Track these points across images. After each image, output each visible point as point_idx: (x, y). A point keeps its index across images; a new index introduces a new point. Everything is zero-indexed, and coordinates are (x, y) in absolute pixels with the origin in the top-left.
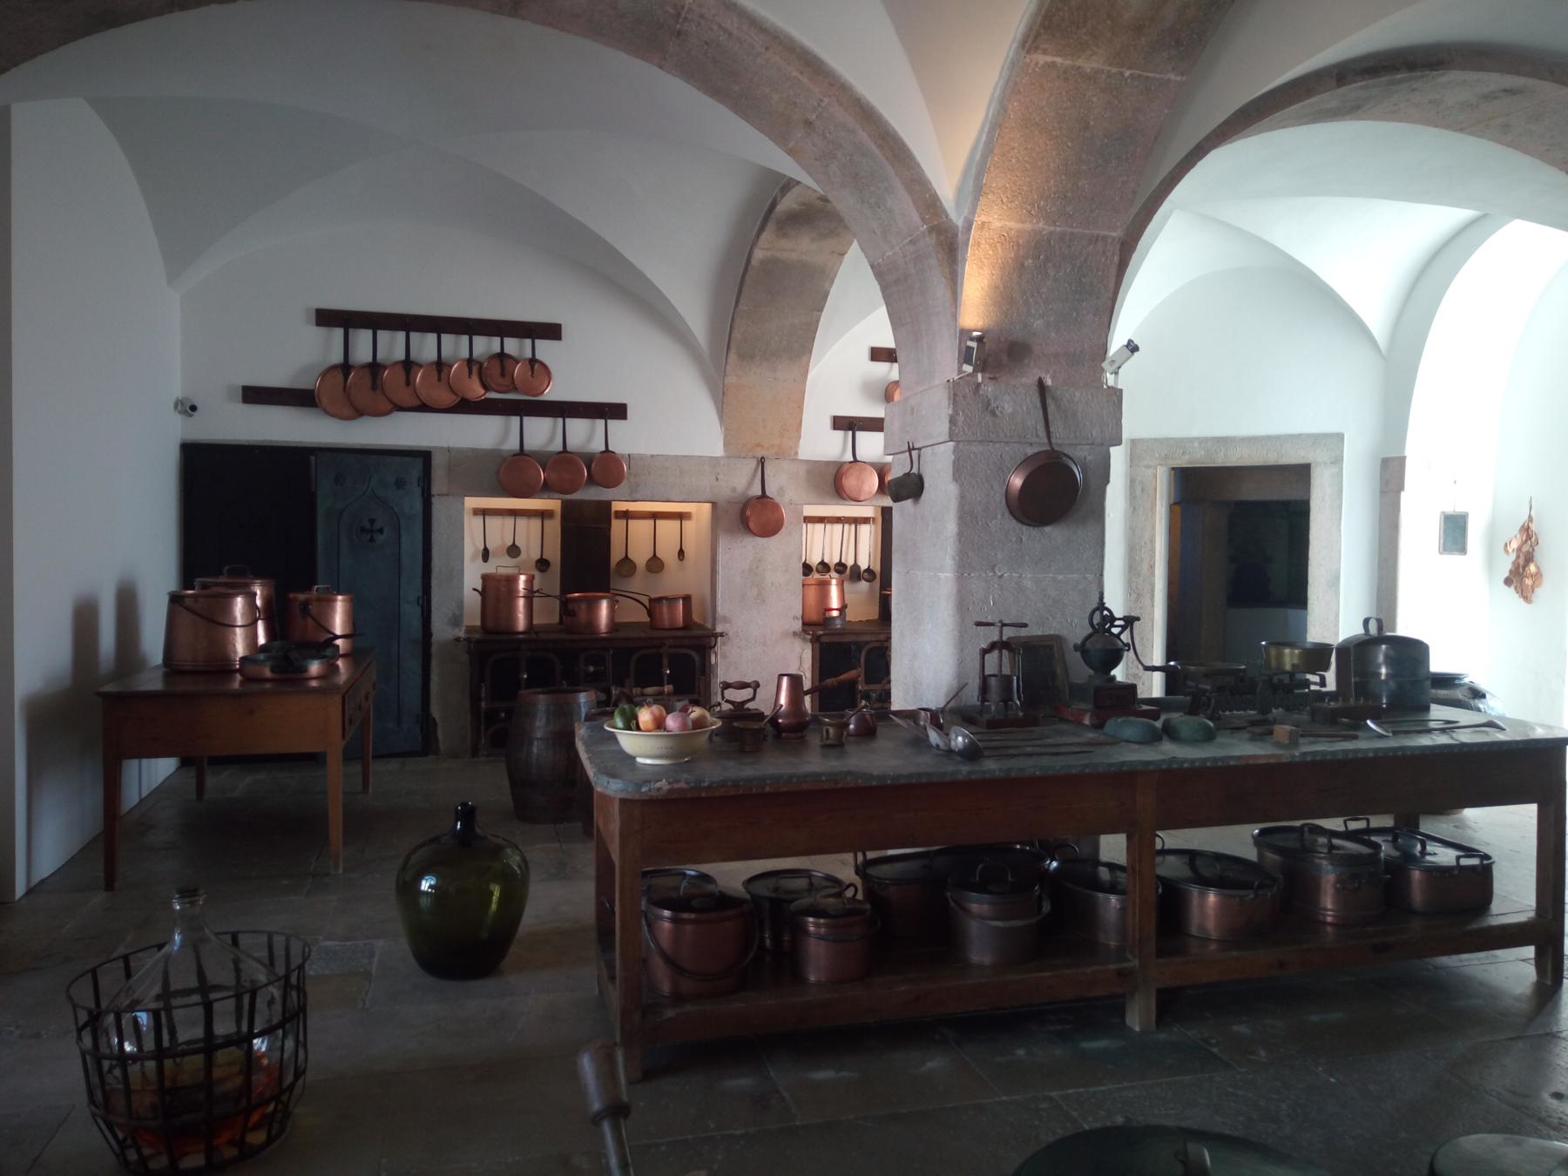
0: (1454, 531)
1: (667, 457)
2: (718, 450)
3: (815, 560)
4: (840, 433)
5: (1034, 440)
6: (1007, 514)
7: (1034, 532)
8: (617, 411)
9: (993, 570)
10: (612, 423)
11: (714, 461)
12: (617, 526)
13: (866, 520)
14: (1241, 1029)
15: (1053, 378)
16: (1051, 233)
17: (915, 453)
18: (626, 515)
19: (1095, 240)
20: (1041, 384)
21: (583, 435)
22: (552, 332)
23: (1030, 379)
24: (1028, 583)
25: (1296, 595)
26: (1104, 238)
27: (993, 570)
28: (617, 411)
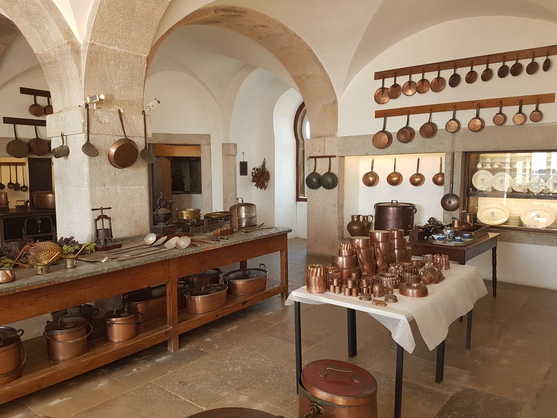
0: (244, 167)
5: (118, 134)
6: (109, 163)
9: (104, 186)
14: (208, 340)
15: (123, 109)
16: (120, 51)
17: (64, 137)
19: (137, 57)
20: (119, 111)
23: (115, 109)
24: (119, 191)
25: (196, 188)
26: (141, 57)
27: (104, 186)
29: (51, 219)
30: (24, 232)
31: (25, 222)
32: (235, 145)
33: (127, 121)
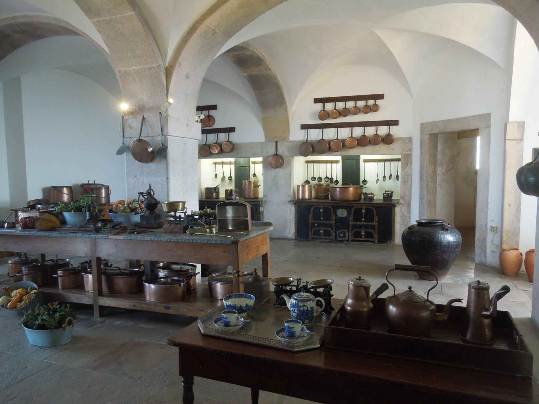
1: (247, 143)
2: (262, 139)
3: (317, 176)
4: (303, 130)
7: (145, 165)
8: (232, 130)
10: (232, 134)
11: (261, 143)
12: (252, 166)
13: (337, 162)
18: (254, 163)
19: (151, 68)
20: (143, 117)
21: (223, 137)
22: (214, 107)
26: (154, 67)
28: (232, 130)
29: (332, 209)
30: (310, 218)
31: (312, 209)
32: (522, 125)
33: (149, 124)
